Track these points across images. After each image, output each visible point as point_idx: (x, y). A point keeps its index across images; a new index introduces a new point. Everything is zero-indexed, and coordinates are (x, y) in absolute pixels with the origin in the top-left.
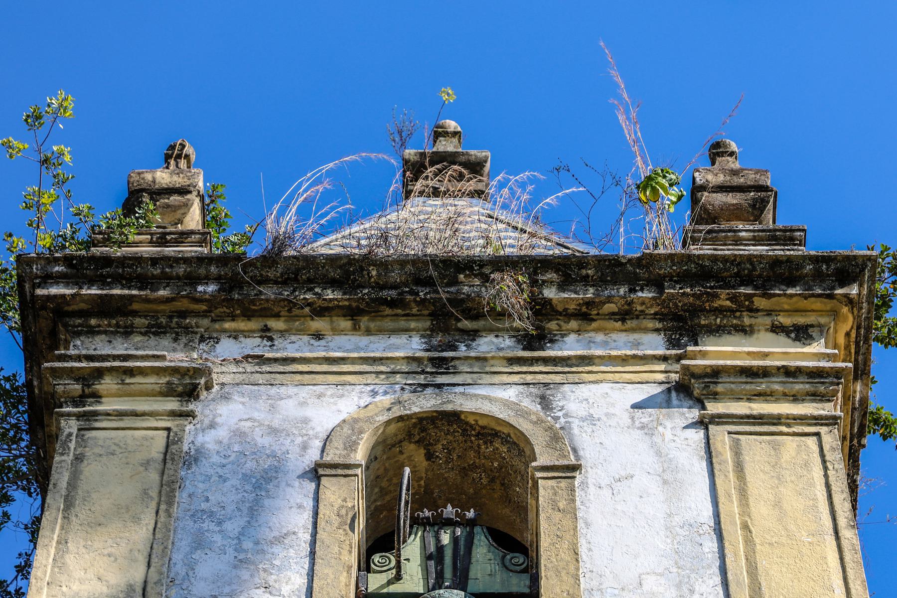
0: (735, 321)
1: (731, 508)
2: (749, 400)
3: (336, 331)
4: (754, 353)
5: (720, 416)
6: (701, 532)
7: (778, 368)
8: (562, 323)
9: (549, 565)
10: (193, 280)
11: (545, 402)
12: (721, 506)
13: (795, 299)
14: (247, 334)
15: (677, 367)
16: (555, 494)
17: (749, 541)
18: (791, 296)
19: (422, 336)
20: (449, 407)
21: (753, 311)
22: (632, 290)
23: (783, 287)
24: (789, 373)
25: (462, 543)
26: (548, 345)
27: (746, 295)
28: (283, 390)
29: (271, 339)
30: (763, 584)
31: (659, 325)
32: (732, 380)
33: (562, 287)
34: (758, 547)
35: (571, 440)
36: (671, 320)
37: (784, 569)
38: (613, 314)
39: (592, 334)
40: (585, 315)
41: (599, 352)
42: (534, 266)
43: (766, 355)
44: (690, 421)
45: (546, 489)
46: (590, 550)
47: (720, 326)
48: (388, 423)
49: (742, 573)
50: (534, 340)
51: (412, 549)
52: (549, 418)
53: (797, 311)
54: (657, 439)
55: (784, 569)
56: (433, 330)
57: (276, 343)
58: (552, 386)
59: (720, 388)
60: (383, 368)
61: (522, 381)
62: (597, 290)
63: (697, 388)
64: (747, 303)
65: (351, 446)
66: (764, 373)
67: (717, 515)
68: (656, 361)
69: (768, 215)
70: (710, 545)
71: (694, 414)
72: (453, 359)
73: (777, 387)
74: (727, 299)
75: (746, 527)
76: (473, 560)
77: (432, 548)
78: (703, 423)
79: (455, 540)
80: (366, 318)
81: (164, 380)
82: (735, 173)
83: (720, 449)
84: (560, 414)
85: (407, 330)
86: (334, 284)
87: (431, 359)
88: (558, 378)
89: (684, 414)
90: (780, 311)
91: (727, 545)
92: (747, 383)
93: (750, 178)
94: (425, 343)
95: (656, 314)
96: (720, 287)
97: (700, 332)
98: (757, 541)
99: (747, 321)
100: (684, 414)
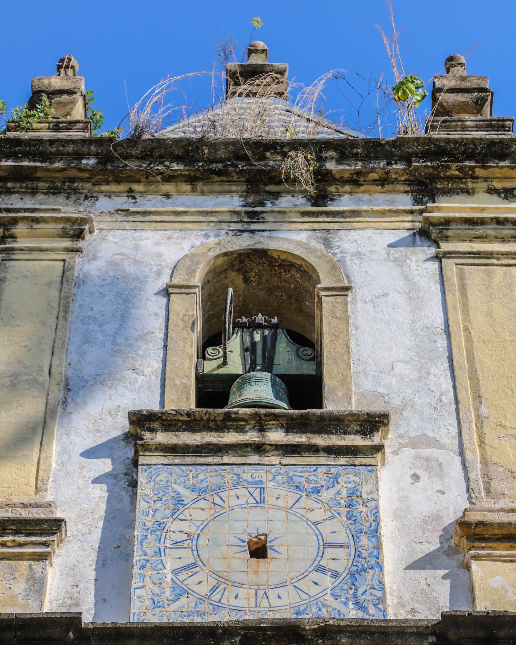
0: (461, 186)
1: (457, 317)
2: (470, 241)
3: (180, 193)
4: (474, 208)
5: (450, 253)
6: (435, 333)
7: (492, 219)
8: (339, 187)
9: (330, 356)
10: (79, 156)
11: (327, 243)
12: (450, 315)
13: (504, 170)
14: (118, 194)
15: (420, 218)
16: (334, 306)
17: (469, 340)
18: (502, 167)
19: (241, 196)
20: (260, 247)
21: (474, 178)
22: (389, 164)
23: (497, 161)
24: (499, 222)
25: (269, 340)
26: (329, 202)
27: (470, 167)
28: (143, 234)
29: (134, 198)
30: (478, 369)
31: (408, 189)
32: (459, 227)
33: (339, 161)
34: (475, 343)
35: (345, 270)
36: (417, 185)
37: (493, 359)
38: (376, 180)
39: (360, 195)
40: (355, 181)
41: (365, 208)
42: (319, 147)
43: (483, 210)
44: (429, 256)
45: (328, 303)
46: (358, 345)
47: (451, 189)
48: (217, 257)
49: (464, 361)
50: (320, 198)
51: (234, 344)
52: (330, 254)
53: (506, 178)
55: (493, 359)
56: (248, 192)
57: (138, 200)
58: (332, 231)
59: (450, 233)
60: (213, 219)
61: (311, 228)
62: (364, 163)
63: (434, 232)
64: (470, 173)
65: (191, 273)
66: (482, 222)
67: (447, 322)
68: (405, 214)
69: (487, 109)
70: (442, 342)
71: (432, 251)
72: (262, 212)
73: (491, 232)
74: (456, 170)
75: (467, 330)
76: (277, 352)
77: (248, 344)
78: (438, 258)
79: (264, 338)
80: (200, 184)
81: (60, 226)
82: (463, 79)
83: (450, 276)
84: (337, 251)
85: (230, 192)
87: (247, 213)
88: (336, 226)
89: (424, 251)
90: (494, 178)
91: (453, 342)
92: (469, 229)
93: (474, 83)
94: (243, 201)
95: (406, 180)
96: (452, 161)
97: (437, 193)
98: (475, 339)
99: (470, 185)
100: (424, 251)
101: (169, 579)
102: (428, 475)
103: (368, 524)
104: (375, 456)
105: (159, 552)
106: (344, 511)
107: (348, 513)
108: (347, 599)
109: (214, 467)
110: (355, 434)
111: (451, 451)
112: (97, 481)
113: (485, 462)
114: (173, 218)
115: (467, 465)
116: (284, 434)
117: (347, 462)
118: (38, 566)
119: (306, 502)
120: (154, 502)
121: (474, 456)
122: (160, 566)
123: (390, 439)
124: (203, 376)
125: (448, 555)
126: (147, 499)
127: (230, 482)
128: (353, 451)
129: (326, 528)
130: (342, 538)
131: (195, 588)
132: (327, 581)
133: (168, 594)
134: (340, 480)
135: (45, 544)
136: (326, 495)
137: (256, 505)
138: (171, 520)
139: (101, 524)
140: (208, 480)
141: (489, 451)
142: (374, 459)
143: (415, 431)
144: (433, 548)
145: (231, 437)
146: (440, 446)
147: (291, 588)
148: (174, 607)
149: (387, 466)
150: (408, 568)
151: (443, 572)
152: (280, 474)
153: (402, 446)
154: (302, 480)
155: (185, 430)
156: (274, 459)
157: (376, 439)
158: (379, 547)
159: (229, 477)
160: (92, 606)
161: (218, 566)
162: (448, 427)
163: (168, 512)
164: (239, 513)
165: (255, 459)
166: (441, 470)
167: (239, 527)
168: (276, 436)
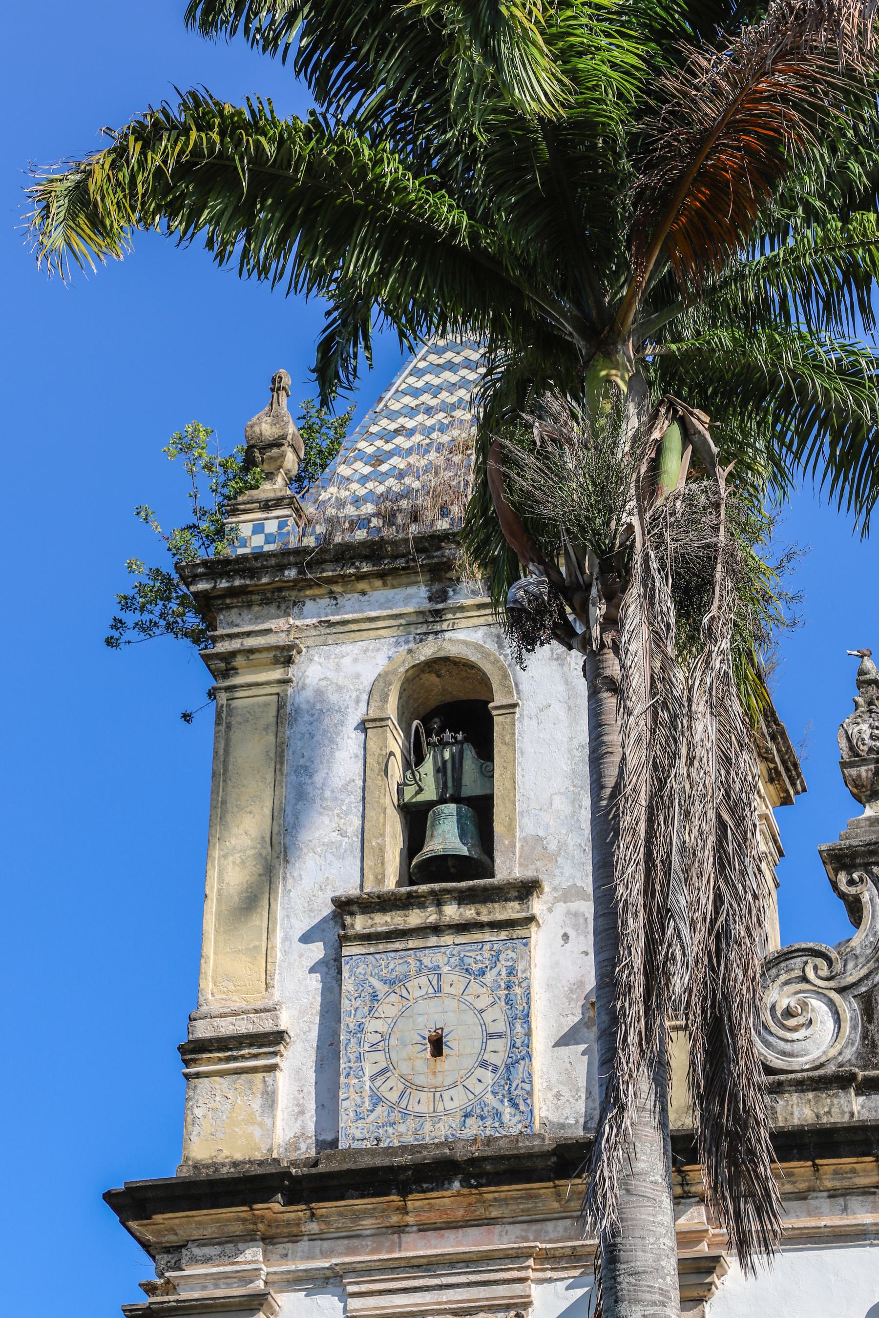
10: (281, 568)
14: (321, 597)
16: (504, 729)
20: (442, 654)
29: (335, 598)
48: (407, 671)
54: (566, 669)
60: (403, 621)
72: (443, 609)
81: (271, 655)
86: (366, 558)
101: (367, 1088)
103: (521, 1008)
105: (359, 1059)
107: (506, 995)
108: (503, 1096)
109: (402, 953)
112: (312, 970)
114: (367, 625)
118: (269, 1077)
119: (474, 988)
122: (361, 1073)
124: (405, 804)
125: (588, 1027)
128: (510, 924)
130: (501, 1027)
131: (388, 1095)
132: (488, 1077)
133: (367, 1105)
135: (275, 1054)
136: (490, 977)
138: (368, 1018)
139: (318, 1018)
144: (577, 1020)
145: (415, 918)
147: (460, 1087)
148: (372, 1117)
149: (543, 926)
150: (557, 1045)
151: (583, 1047)
153: (556, 900)
155: (379, 911)
156: (448, 939)
158: (529, 1034)
160: (313, 1112)
161: (404, 1068)
163: (366, 1009)
164: (422, 1006)
165: (433, 941)
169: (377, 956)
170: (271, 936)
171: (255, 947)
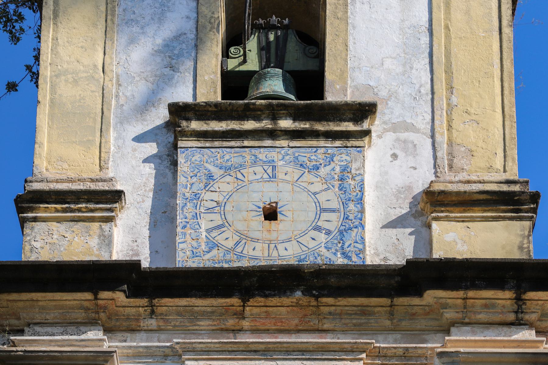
102: (404, 154)
103: (355, 194)
104: (363, 139)
106: (337, 184)
107: (340, 185)
110: (348, 121)
111: (424, 134)
112: (146, 161)
113: (450, 143)
115: (436, 146)
116: (292, 121)
117: (341, 144)
119: (308, 177)
120: (191, 177)
121: (442, 139)
123: (376, 125)
126: (185, 175)
127: (249, 161)
128: (346, 135)
129: (322, 197)
130: (334, 204)
134: (335, 159)
136: (323, 171)
137: (269, 180)
140: (232, 160)
141: (455, 134)
142: (362, 142)
143: (397, 118)
146: (415, 130)
149: (373, 147)
152: (288, 154)
153: (386, 130)
154: (305, 159)
156: (284, 143)
157: (365, 125)
158: (362, 211)
159: (248, 158)
162: (424, 114)
163: (202, 185)
164: (256, 186)
165: (268, 143)
166: (415, 150)
167: (256, 196)
168: (286, 124)
169: (213, 150)
170: (104, 133)
171: (89, 141)
